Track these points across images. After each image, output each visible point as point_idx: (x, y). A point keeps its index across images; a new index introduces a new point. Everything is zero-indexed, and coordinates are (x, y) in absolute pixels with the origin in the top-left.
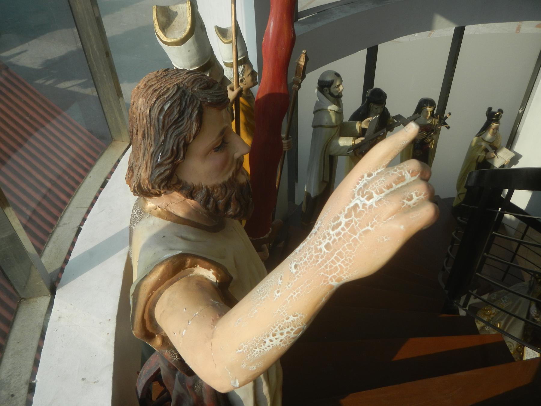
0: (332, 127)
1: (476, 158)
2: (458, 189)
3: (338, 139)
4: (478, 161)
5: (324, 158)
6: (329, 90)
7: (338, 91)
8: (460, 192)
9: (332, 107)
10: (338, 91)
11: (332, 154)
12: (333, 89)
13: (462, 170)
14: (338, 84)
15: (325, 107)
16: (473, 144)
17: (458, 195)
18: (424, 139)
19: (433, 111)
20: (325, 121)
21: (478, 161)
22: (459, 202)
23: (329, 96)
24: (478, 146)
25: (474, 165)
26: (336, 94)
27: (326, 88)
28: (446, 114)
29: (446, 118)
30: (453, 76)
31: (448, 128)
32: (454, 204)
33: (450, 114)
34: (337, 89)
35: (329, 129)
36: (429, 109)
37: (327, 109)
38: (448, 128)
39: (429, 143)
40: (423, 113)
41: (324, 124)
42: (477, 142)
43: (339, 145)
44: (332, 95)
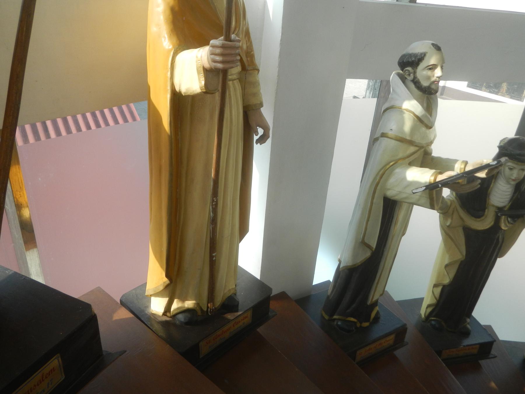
0: (401, 140)
3: (408, 168)
5: (373, 198)
6: (415, 73)
7: (429, 78)
9: (412, 106)
10: (429, 78)
11: (390, 194)
12: (421, 72)
14: (433, 61)
15: (397, 103)
20: (391, 126)
23: (412, 86)
26: (425, 84)
27: (409, 69)
34: (429, 73)
35: (393, 143)
37: (400, 108)
41: (391, 134)
43: (405, 178)
44: (416, 83)
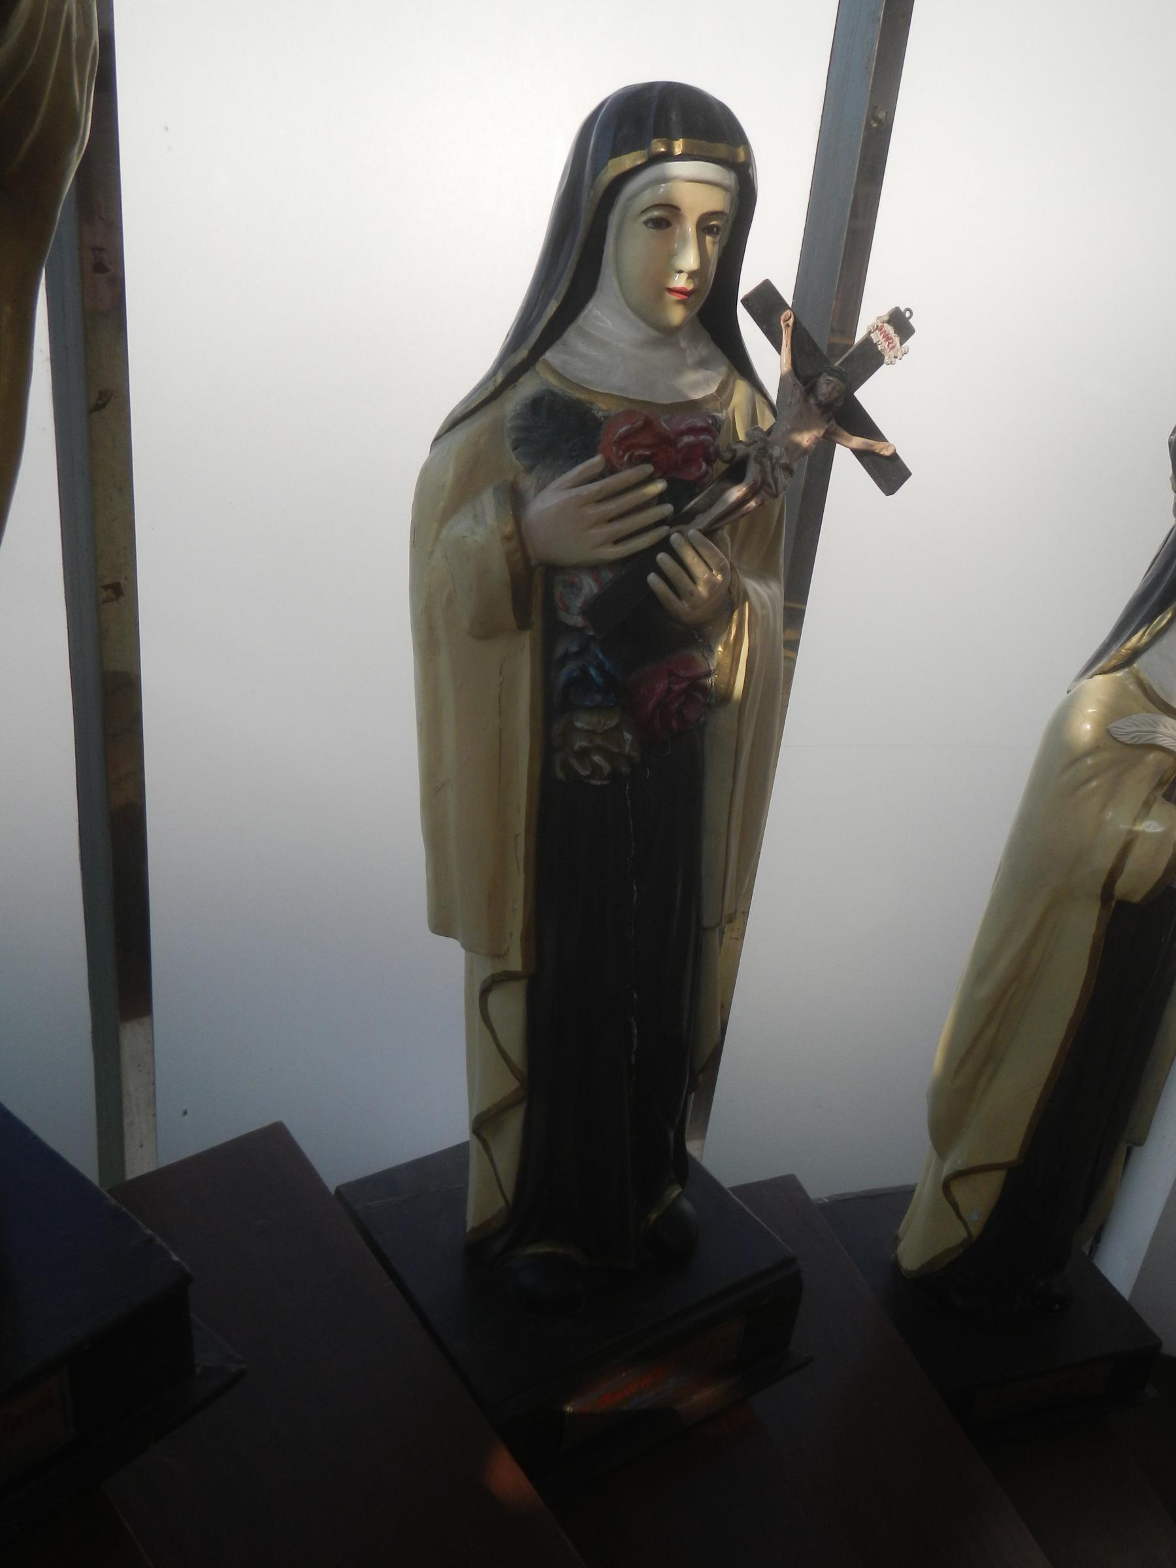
1: (1104, 860)
2: (945, 1129)
4: (1122, 887)
8: (956, 1160)
13: (980, 969)
16: (1085, 728)
17: (946, 1187)
18: (644, 561)
19: (731, 228)
21: (1122, 887)
22: (955, 1235)
24: (1119, 750)
25: (1082, 927)
28: (870, 317)
29: (869, 359)
30: (791, 678)
31: (888, 472)
32: (916, 1244)
33: (900, 324)
36: (691, 182)
38: (888, 472)
39: (697, 634)
40: (629, 245)
42: (1115, 711)
